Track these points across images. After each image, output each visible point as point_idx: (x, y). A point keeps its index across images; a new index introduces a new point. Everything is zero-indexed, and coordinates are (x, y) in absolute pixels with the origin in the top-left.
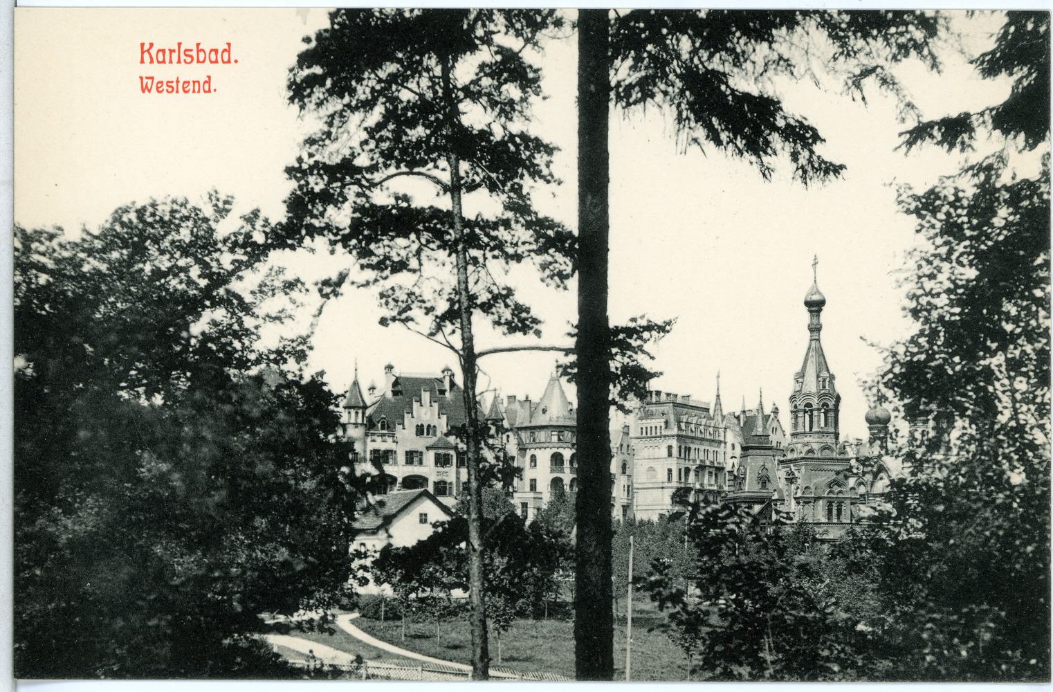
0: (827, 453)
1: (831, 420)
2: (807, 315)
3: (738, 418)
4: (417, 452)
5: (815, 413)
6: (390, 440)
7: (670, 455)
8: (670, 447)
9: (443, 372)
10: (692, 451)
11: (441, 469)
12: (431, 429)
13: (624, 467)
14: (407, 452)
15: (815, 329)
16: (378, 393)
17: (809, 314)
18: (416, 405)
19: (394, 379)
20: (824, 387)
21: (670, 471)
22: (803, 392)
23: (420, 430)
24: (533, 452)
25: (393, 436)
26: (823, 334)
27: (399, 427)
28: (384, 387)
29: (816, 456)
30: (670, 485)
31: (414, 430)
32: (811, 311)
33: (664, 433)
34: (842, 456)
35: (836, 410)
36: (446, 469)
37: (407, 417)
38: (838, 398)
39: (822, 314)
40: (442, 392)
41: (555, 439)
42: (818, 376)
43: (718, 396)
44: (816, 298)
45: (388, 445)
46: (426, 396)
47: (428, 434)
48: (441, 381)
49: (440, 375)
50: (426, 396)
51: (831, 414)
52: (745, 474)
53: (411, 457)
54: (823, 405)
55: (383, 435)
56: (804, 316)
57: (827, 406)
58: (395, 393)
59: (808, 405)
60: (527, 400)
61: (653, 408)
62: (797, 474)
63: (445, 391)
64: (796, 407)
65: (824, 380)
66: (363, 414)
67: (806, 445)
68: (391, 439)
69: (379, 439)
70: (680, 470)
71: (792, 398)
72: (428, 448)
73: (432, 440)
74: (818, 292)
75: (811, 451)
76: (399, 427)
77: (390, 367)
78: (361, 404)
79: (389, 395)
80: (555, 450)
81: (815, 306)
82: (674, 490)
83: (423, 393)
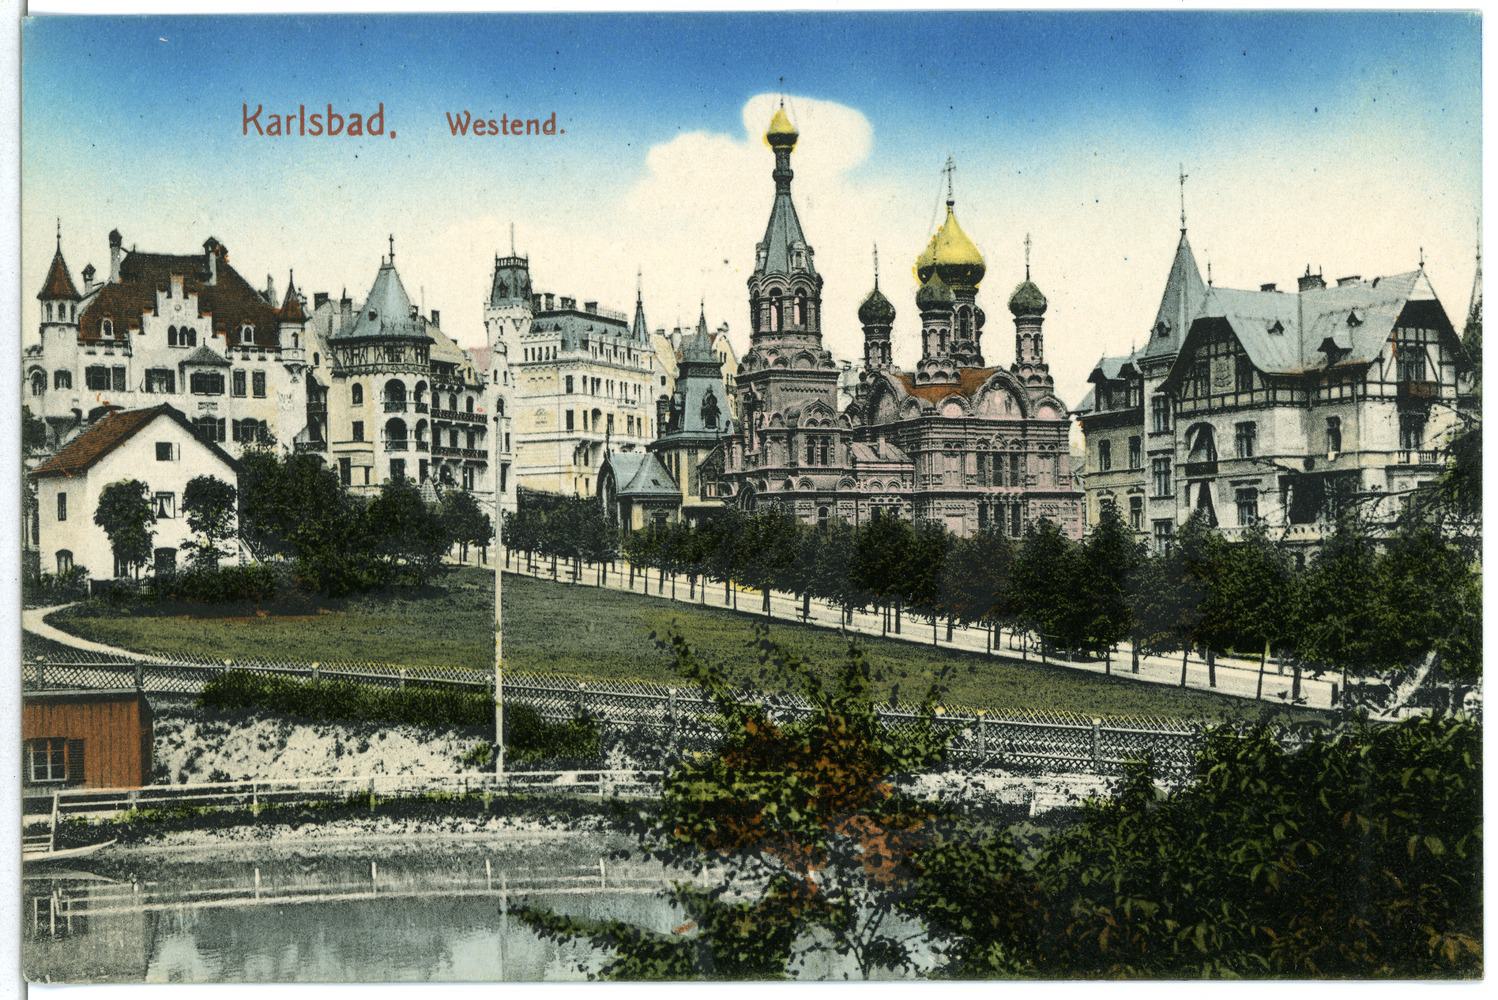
0: (803, 365)
2: (773, 156)
5: (787, 304)
6: (118, 352)
7: (570, 390)
8: (569, 379)
10: (603, 384)
11: (204, 399)
12: (189, 335)
15: (783, 178)
18: (161, 297)
19: (123, 255)
21: (570, 414)
24: (356, 379)
27: (134, 334)
28: (105, 273)
30: (572, 436)
32: (776, 151)
34: (827, 369)
35: (818, 302)
36: (214, 399)
37: (148, 317)
38: (820, 282)
39: (792, 156)
43: (639, 304)
44: (784, 129)
45: (118, 358)
46: (177, 288)
47: (182, 343)
48: (201, 260)
49: (199, 250)
50: (177, 288)
52: (683, 405)
53: (158, 377)
54: (797, 292)
55: (109, 344)
56: (768, 159)
57: (804, 293)
59: (776, 292)
61: (543, 321)
63: (211, 275)
66: (73, 309)
67: (773, 351)
69: (100, 351)
70: (585, 412)
72: (182, 365)
73: (187, 353)
75: (783, 361)
79: (117, 279)
80: (390, 377)
82: (577, 443)
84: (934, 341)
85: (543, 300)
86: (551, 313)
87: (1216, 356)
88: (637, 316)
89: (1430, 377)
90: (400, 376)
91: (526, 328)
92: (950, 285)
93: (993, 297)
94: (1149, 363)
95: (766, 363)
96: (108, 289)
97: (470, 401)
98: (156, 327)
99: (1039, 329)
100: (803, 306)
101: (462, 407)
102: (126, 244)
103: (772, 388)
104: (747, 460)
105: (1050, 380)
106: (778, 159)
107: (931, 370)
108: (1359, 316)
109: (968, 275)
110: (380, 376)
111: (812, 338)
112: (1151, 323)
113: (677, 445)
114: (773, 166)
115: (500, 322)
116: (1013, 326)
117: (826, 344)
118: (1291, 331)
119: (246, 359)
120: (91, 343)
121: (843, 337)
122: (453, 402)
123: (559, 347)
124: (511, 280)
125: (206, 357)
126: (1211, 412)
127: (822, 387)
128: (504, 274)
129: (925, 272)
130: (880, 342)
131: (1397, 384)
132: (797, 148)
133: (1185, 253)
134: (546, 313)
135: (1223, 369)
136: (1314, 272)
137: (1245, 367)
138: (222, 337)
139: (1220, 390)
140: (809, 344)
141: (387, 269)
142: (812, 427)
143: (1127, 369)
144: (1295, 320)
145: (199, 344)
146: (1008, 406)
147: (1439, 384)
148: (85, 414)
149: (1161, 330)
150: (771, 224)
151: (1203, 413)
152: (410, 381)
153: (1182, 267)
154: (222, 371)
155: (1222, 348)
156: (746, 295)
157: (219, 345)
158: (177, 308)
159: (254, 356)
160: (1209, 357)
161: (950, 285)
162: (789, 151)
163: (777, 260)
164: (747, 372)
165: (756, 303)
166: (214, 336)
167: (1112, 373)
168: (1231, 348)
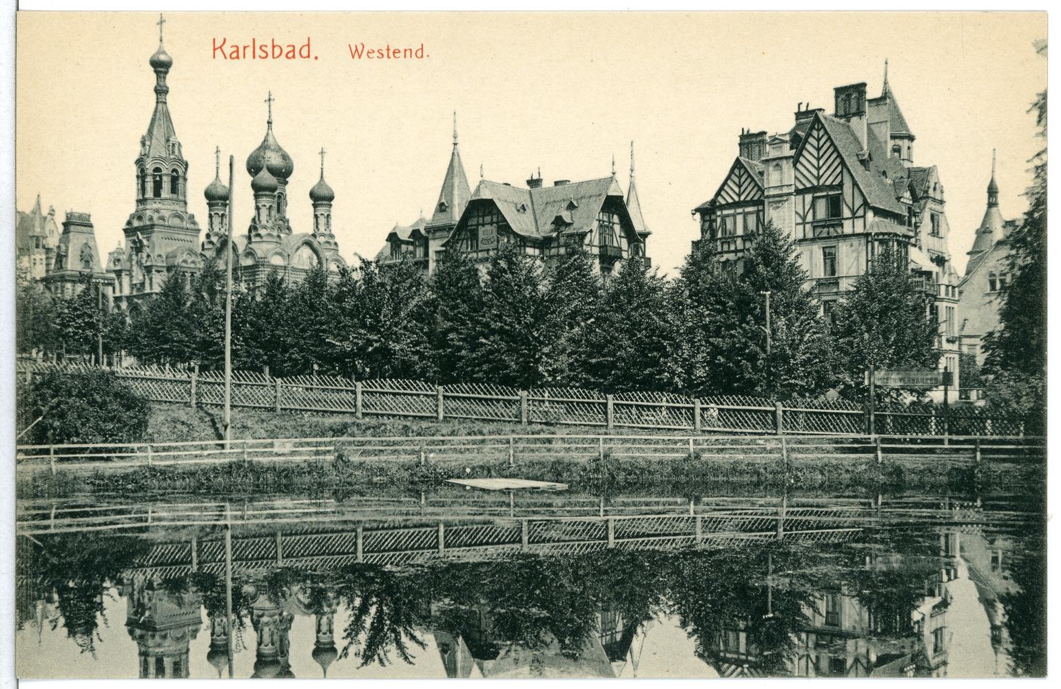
1: (180, 187)
5: (165, 179)
15: (161, 91)
17: (155, 75)
20: (173, 152)
26: (169, 98)
29: (166, 223)
32: (155, 71)
34: (192, 226)
35: (185, 180)
38: (187, 165)
44: (163, 58)
51: (181, 181)
52: (67, 251)
56: (151, 77)
62: (145, 242)
64: (142, 171)
65: (173, 145)
67: (157, 211)
71: (140, 162)
74: (164, 53)
75: (162, 218)
81: (161, 67)
84: (264, 212)
87: (483, 225)
89: (615, 244)
92: (270, 175)
94: (433, 230)
95: (151, 219)
99: (329, 211)
100: (174, 180)
103: (154, 237)
104: (132, 286)
105: (336, 244)
106: (158, 78)
107: (263, 232)
108: (575, 203)
109: (283, 174)
111: (182, 204)
113: (63, 279)
114: (155, 83)
116: (312, 209)
118: (529, 211)
127: (188, 238)
129: (254, 167)
130: (220, 213)
131: (600, 247)
132: (171, 70)
133: (456, 157)
135: (486, 232)
136: (535, 177)
137: (504, 228)
139: (486, 247)
140: (179, 208)
142: (184, 265)
143: (415, 233)
144: (530, 205)
146: (310, 258)
147: (620, 249)
149: (442, 208)
150: (153, 120)
153: (453, 170)
155: (488, 219)
156: (134, 171)
160: (478, 225)
162: (166, 73)
164: (136, 224)
165: (142, 177)
167: (404, 236)
168: (495, 220)
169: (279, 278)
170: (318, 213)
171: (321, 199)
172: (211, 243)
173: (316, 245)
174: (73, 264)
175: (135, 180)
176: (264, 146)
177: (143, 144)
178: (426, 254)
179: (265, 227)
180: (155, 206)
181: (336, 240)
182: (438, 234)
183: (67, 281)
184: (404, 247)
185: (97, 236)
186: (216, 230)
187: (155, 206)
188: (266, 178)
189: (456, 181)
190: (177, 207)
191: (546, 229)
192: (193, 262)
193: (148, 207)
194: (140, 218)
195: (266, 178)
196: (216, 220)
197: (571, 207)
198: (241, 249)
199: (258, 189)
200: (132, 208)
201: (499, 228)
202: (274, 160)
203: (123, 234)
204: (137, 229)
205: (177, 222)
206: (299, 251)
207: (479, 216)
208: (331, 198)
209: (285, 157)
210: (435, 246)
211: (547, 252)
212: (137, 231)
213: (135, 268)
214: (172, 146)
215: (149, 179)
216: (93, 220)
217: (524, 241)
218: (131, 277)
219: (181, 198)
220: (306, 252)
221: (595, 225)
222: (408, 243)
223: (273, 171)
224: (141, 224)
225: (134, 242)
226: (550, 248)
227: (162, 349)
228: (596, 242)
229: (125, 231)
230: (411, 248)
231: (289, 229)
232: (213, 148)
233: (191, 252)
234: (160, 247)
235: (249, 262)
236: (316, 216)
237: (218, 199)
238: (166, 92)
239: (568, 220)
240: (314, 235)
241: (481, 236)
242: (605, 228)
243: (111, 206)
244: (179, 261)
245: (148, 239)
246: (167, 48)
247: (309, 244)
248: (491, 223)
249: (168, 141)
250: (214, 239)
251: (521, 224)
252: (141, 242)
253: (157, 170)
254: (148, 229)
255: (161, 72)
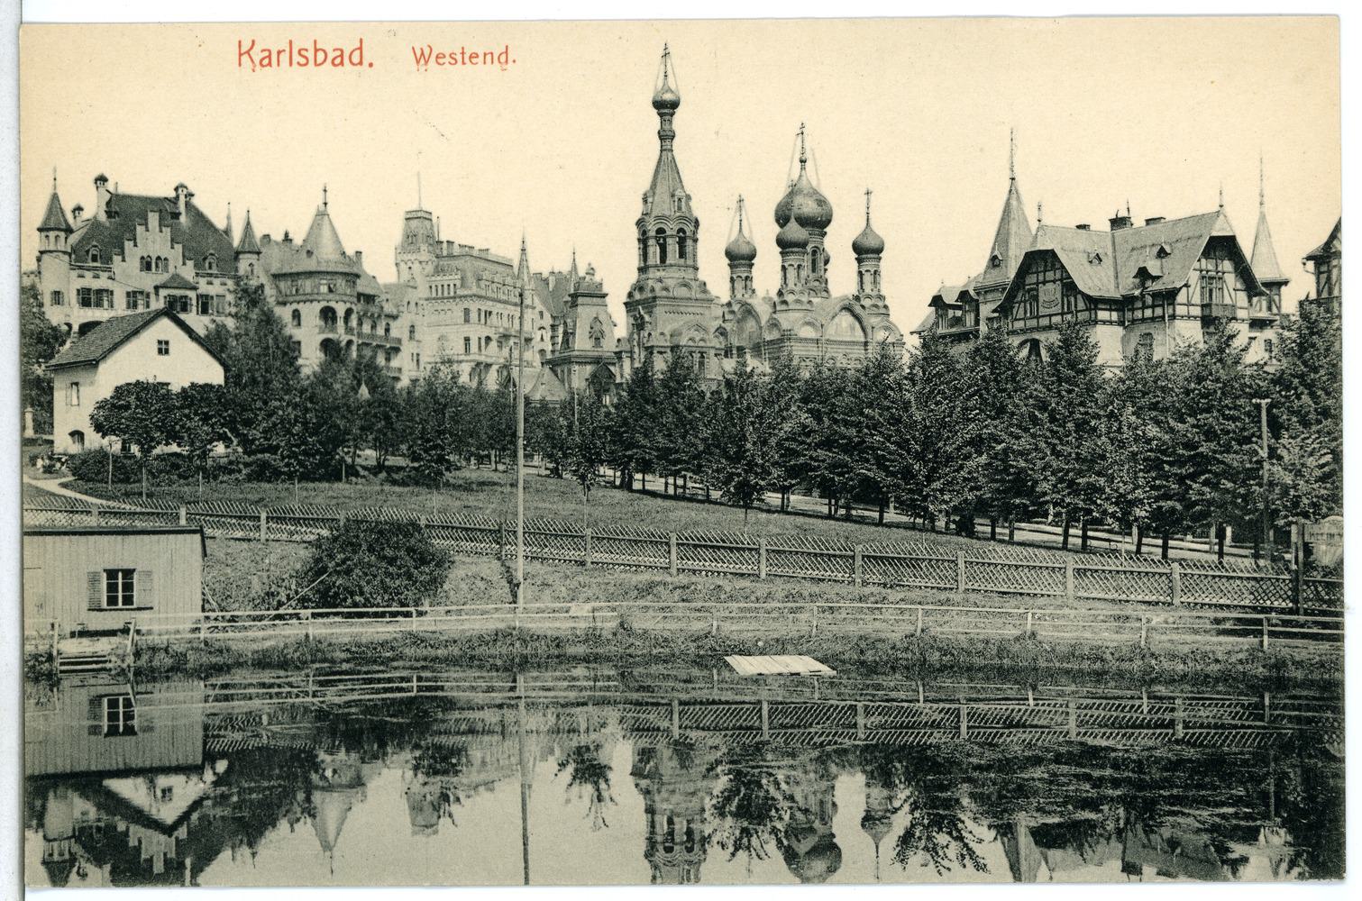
0: (683, 292)
1: (689, 249)
3: (546, 281)
4: (142, 293)
5: (669, 241)
6: (104, 275)
7: (467, 320)
8: (467, 311)
9: (176, 189)
10: (494, 316)
13: (412, 330)
14: (128, 294)
15: (666, 136)
16: (87, 214)
18: (140, 229)
20: (680, 208)
21: (467, 340)
22: (654, 214)
23: (146, 265)
24: (295, 306)
25: (109, 270)
27: (117, 259)
28: (93, 206)
31: (137, 264)
33: (460, 292)
35: (696, 241)
37: (128, 245)
38: (697, 223)
40: (176, 216)
41: (324, 289)
42: (673, 196)
43: (523, 250)
44: (668, 97)
46: (153, 219)
47: (157, 266)
49: (172, 194)
50: (153, 219)
51: (689, 242)
55: (95, 269)
56: (654, 120)
57: (684, 232)
58: (109, 214)
60: (287, 239)
61: (444, 262)
62: (647, 318)
64: (644, 233)
67: (660, 280)
68: (106, 274)
69: (89, 274)
71: (640, 223)
73: (162, 278)
75: (666, 289)
76: (117, 259)
77: (102, 179)
78: (64, 227)
79: (103, 217)
80: (324, 304)
81: (666, 108)
82: (473, 364)
83: (150, 215)
84: (791, 273)
85: (445, 245)
86: (450, 256)
87: (1044, 283)
88: (522, 260)
90: (332, 304)
91: (430, 268)
92: (803, 227)
93: (838, 242)
94: (984, 291)
95: (653, 290)
96: (94, 224)
97: (387, 330)
98: (133, 253)
100: (682, 243)
101: (380, 331)
102: (110, 186)
103: (658, 311)
105: (886, 307)
107: (790, 298)
109: (819, 224)
110: (315, 303)
112: (987, 256)
113: (568, 361)
114: (659, 127)
115: (410, 264)
117: (702, 276)
118: (1108, 262)
119: (210, 283)
120: (80, 268)
121: (713, 272)
122: (374, 327)
123: (458, 283)
124: (419, 232)
125: (177, 282)
126: (1038, 329)
128: (414, 223)
129: (782, 218)
130: (744, 275)
132: (679, 111)
134: (444, 255)
135: (1050, 292)
137: (1070, 287)
138: (190, 263)
139: (1048, 311)
140: (689, 275)
141: (322, 214)
142: (691, 343)
143: (964, 295)
144: (1110, 252)
145: (171, 269)
146: (853, 329)
148: (76, 328)
149: (994, 262)
151: (1032, 330)
152: (340, 309)
154: (192, 294)
155: (1050, 275)
157: (188, 272)
158: (153, 239)
159: (217, 282)
160: (1037, 284)
161: (803, 227)
162: (672, 115)
163: (663, 206)
164: (637, 296)
165: (643, 241)
166: (184, 264)
167: (950, 299)
169: (749, 369)
170: (863, 270)
171: (867, 252)
172: (733, 312)
173: (858, 309)
174: (582, 343)
175: (636, 244)
176: (794, 191)
177: (645, 201)
178: (977, 322)
179: (792, 292)
180: (658, 274)
181: (887, 302)
182: (989, 297)
183: (571, 362)
184: (951, 313)
185: (610, 309)
186: (739, 296)
187: (658, 274)
188: (795, 231)
189: (1013, 227)
190: (683, 274)
191: (1128, 285)
192: (702, 340)
193: (651, 276)
194: (641, 289)
195: (795, 231)
196: (739, 285)
197: (1162, 254)
198: (764, 319)
199: (785, 245)
200: (633, 276)
201: (1064, 285)
202: (808, 207)
203: (623, 308)
204: (638, 303)
205: (683, 292)
206: (836, 320)
207: (1037, 273)
208: (879, 250)
209: (821, 202)
210: (986, 310)
211: (1128, 315)
212: (640, 304)
213: (636, 350)
214: (681, 200)
215: (651, 242)
216: (605, 290)
217: (1094, 303)
218: (632, 359)
219: (690, 262)
220: (846, 320)
221: (1194, 277)
222: (959, 308)
223: (804, 221)
224: (644, 296)
225: (635, 318)
226: (1133, 310)
227: (625, 456)
228: (1197, 299)
229: (626, 304)
230: (959, 313)
231: (826, 291)
232: (733, 201)
233: (699, 327)
234: (664, 325)
235: (775, 335)
236: (860, 274)
237: (740, 259)
238: (673, 137)
239: (1154, 272)
240: (857, 298)
241: (1042, 298)
242: (1209, 280)
243: (618, 273)
244: (684, 341)
245: (650, 313)
246: (671, 83)
247: (848, 309)
248: (1054, 281)
249: (673, 196)
250: (736, 308)
251: (1093, 281)
252: (642, 317)
253: (660, 231)
254: (650, 304)
255: (665, 114)
